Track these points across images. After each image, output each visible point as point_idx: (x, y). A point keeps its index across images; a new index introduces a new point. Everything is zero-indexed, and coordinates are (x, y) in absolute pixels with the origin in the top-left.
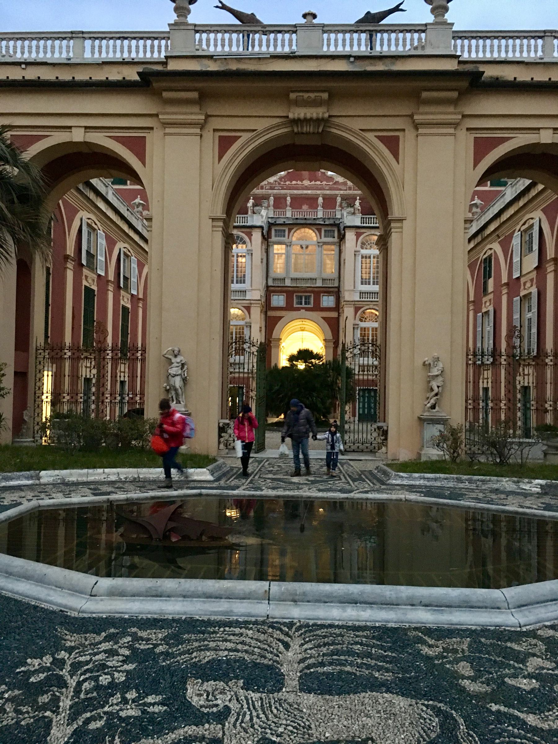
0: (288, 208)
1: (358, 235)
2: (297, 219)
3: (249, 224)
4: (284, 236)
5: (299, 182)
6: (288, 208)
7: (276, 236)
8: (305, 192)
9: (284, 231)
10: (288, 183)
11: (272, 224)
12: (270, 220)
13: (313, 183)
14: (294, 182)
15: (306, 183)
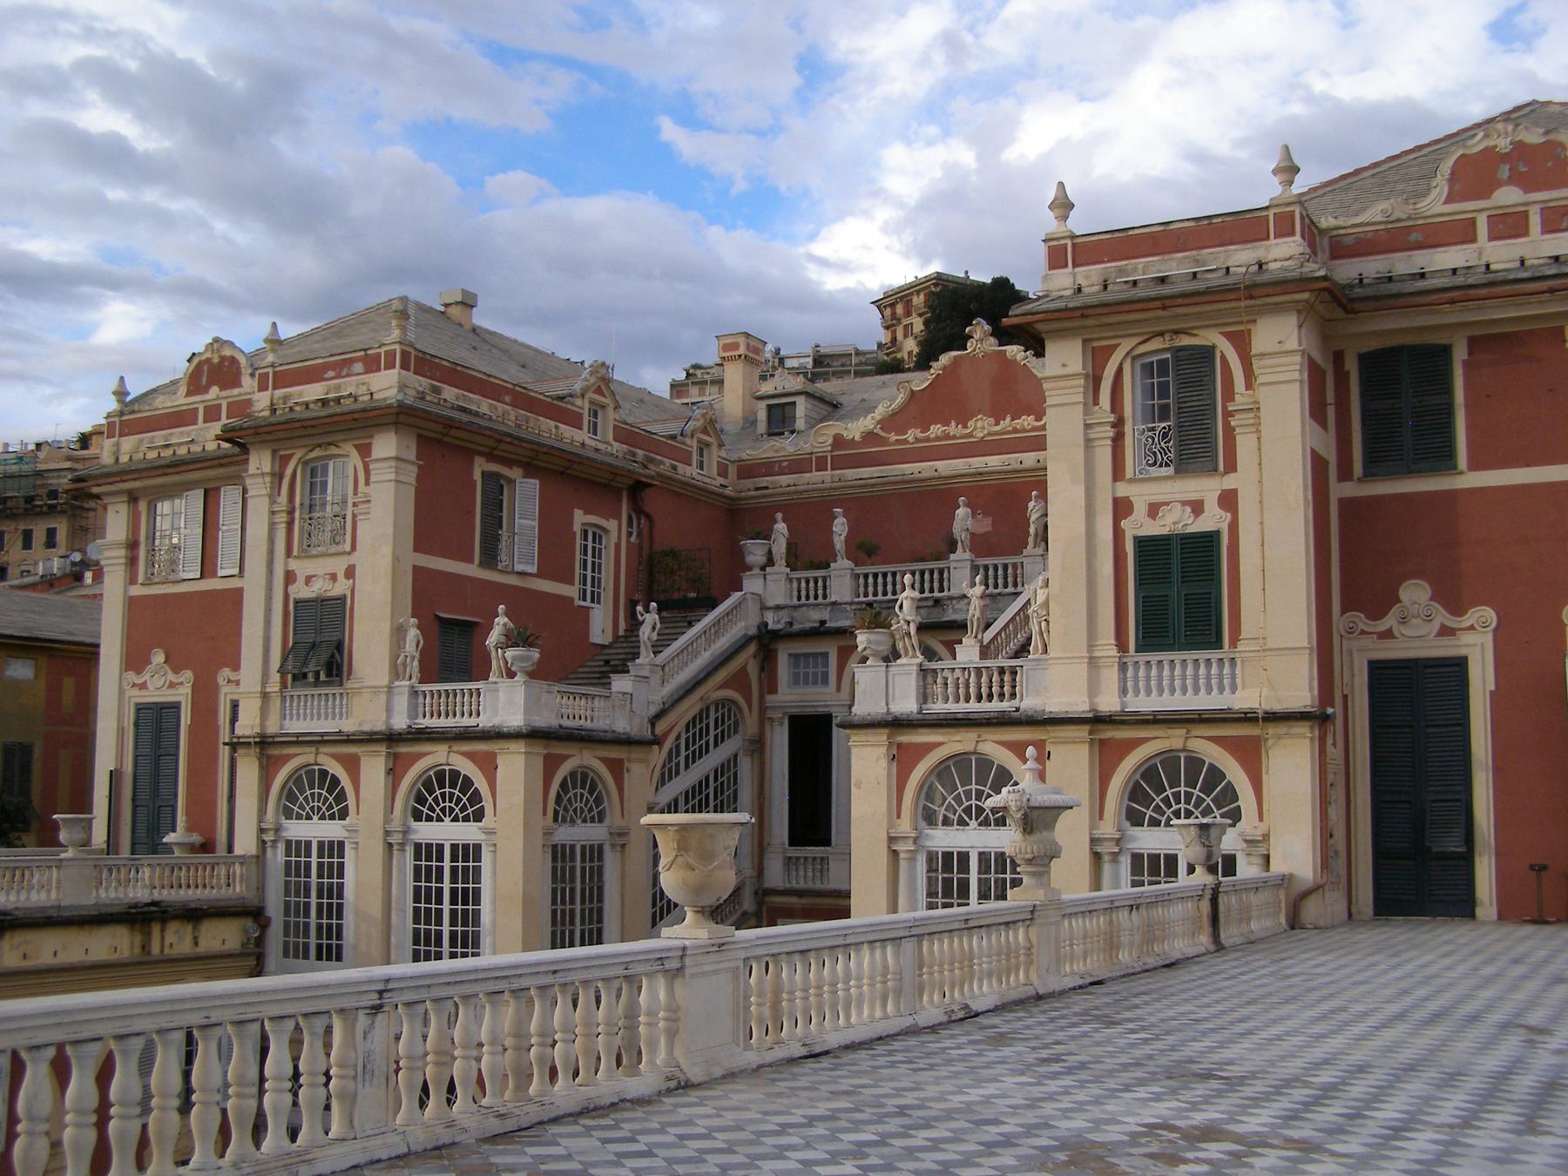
0: (842, 565)
1: (903, 759)
2: (870, 604)
3: (485, 721)
4: (825, 681)
5: (954, 429)
6: (842, 565)
7: (795, 681)
8: (977, 463)
9: (826, 655)
10: (911, 434)
11: (776, 636)
12: (770, 618)
13: (1006, 423)
14: (936, 430)
15: (981, 426)
